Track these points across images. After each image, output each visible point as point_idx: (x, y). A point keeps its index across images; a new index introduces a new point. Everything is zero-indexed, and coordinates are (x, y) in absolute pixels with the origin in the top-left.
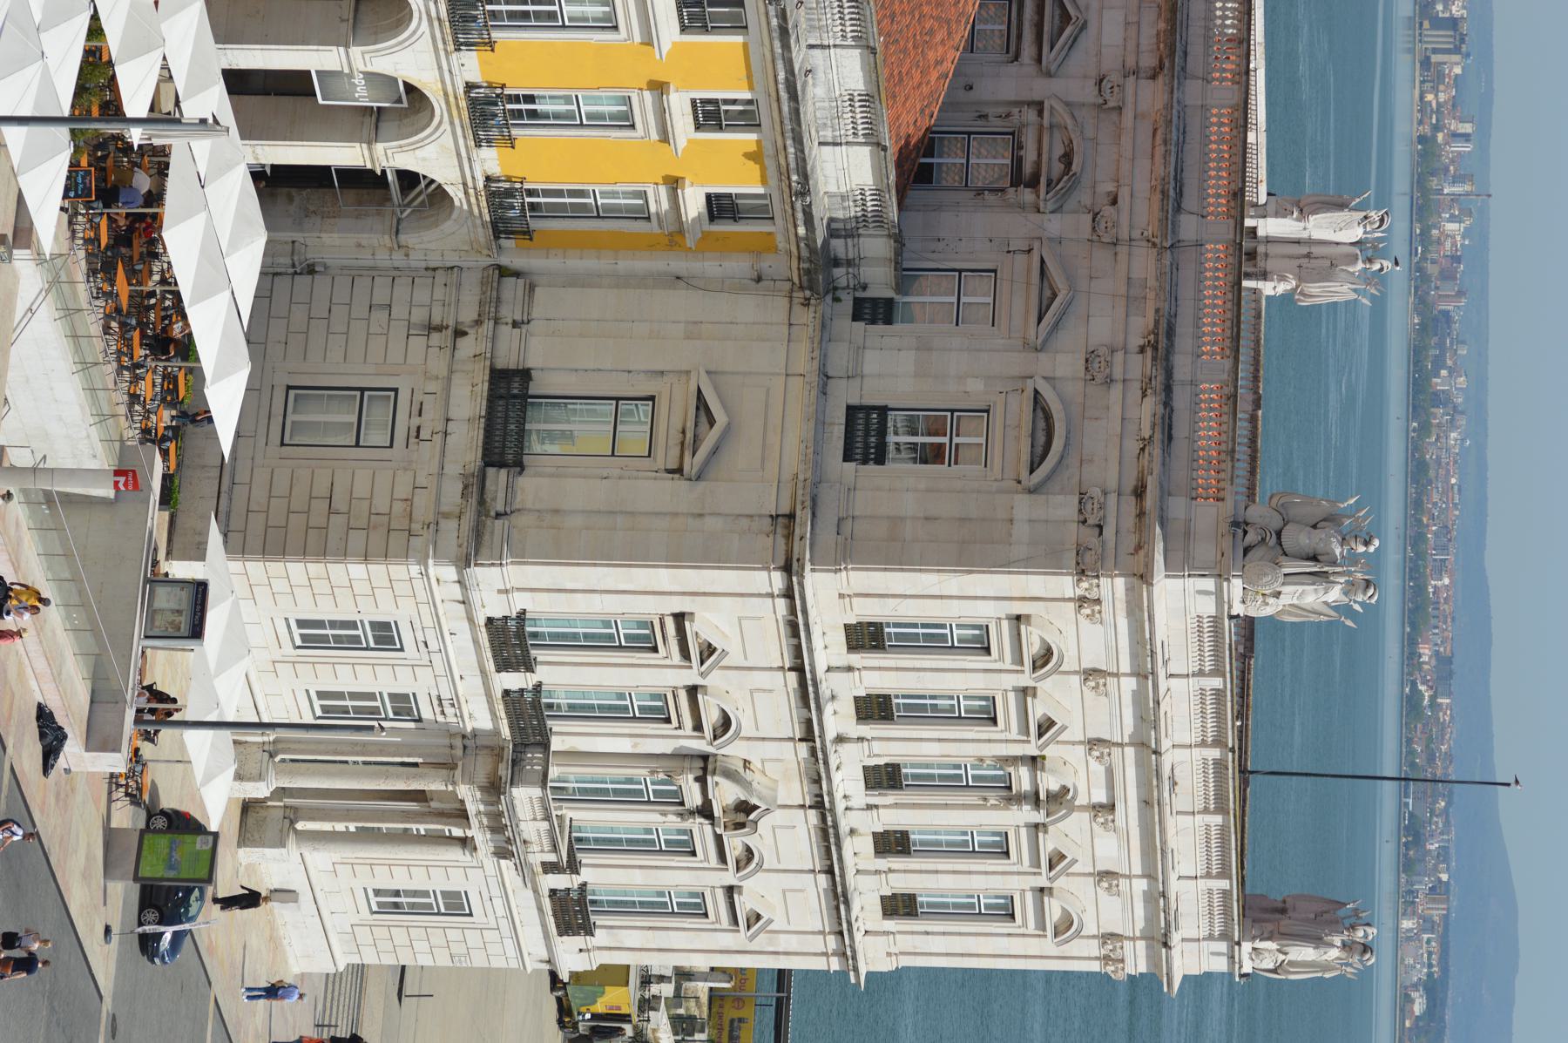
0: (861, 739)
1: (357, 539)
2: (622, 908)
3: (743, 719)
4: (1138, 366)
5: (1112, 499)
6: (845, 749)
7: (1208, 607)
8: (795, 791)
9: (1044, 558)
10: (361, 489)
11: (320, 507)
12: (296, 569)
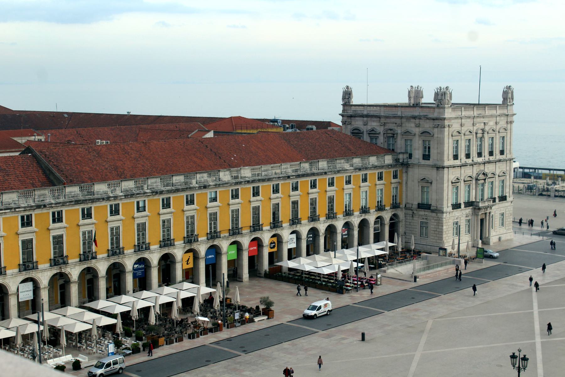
0: (473, 158)
1: (440, 227)
2: (503, 191)
3: (470, 174)
4: (417, 121)
5: (434, 123)
6: (474, 160)
7: (450, 110)
8: (482, 167)
9: (442, 133)
10: (433, 227)
11: (436, 232)
12: (444, 236)
